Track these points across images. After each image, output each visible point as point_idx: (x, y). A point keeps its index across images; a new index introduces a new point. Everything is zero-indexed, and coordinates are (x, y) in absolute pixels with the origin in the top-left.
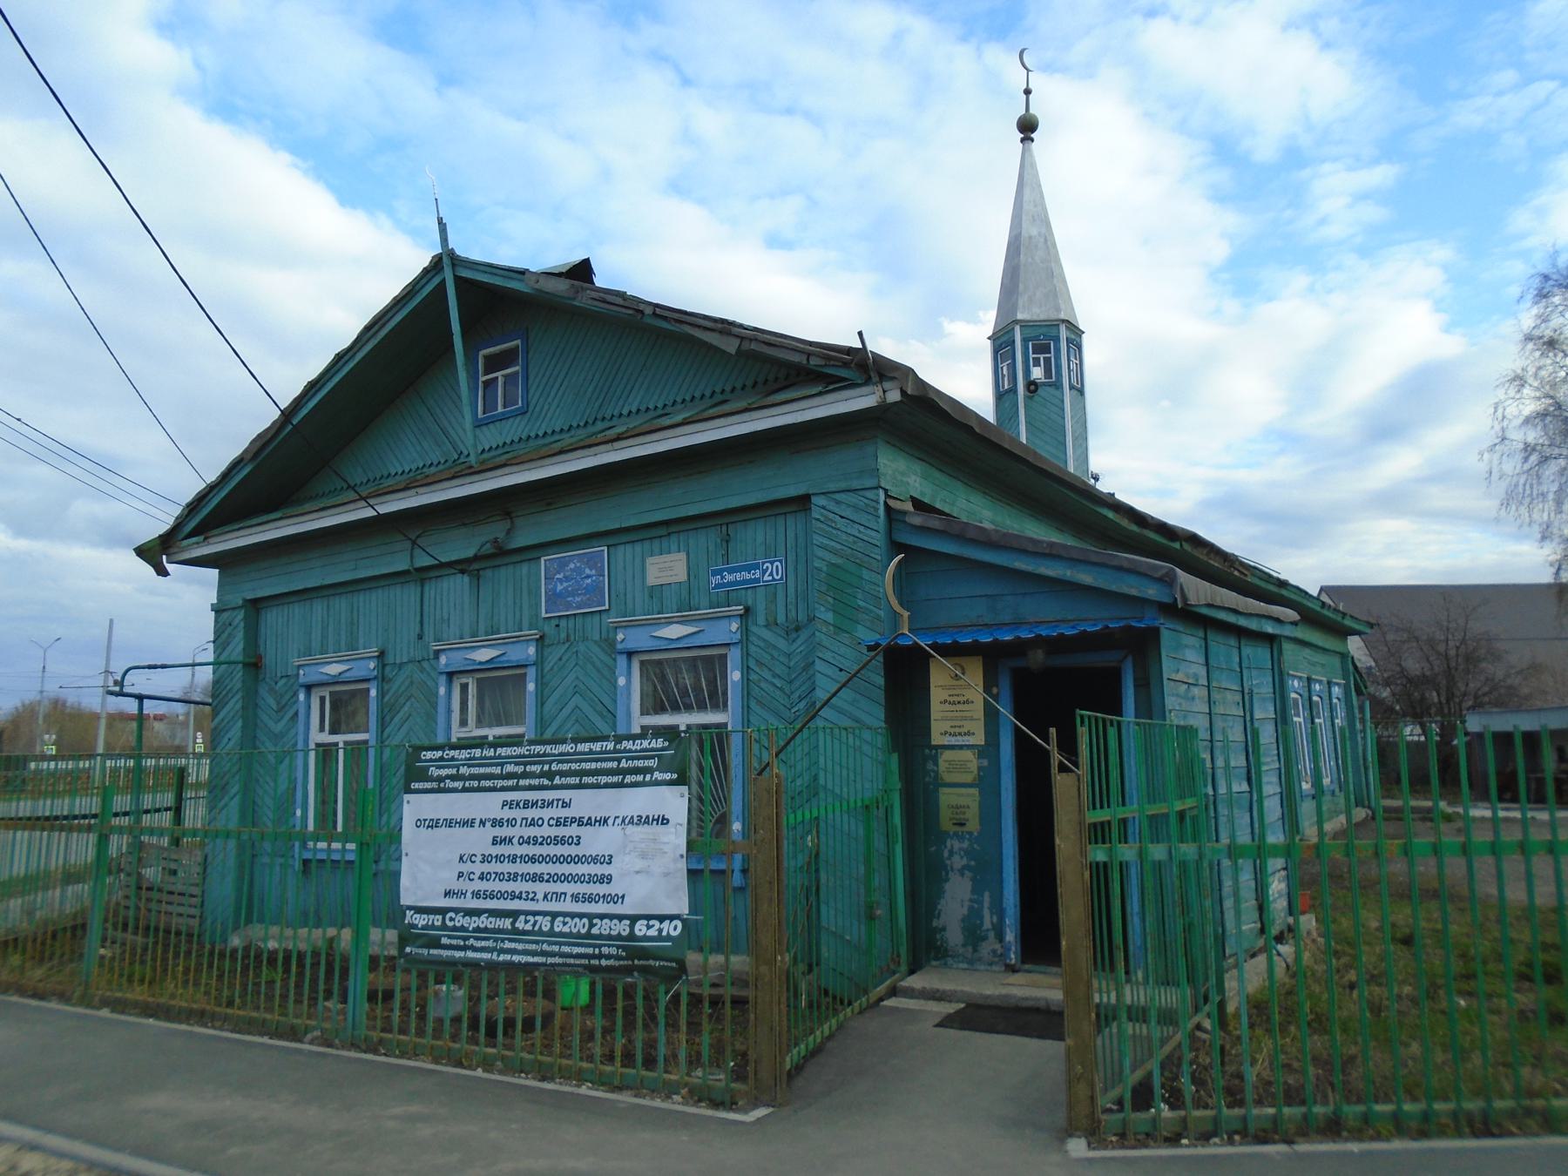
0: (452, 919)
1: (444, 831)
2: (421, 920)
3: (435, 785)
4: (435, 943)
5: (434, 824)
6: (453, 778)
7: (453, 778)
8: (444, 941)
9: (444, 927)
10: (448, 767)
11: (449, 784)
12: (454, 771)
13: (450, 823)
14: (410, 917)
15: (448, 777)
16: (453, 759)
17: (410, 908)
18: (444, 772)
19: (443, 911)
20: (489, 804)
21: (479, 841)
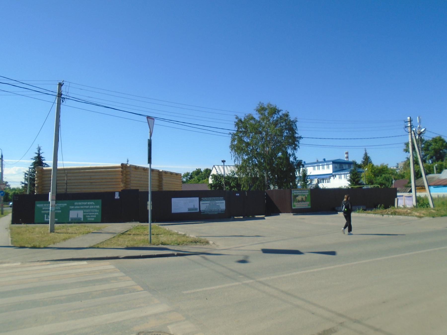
20: (209, 202)
21: (208, 205)
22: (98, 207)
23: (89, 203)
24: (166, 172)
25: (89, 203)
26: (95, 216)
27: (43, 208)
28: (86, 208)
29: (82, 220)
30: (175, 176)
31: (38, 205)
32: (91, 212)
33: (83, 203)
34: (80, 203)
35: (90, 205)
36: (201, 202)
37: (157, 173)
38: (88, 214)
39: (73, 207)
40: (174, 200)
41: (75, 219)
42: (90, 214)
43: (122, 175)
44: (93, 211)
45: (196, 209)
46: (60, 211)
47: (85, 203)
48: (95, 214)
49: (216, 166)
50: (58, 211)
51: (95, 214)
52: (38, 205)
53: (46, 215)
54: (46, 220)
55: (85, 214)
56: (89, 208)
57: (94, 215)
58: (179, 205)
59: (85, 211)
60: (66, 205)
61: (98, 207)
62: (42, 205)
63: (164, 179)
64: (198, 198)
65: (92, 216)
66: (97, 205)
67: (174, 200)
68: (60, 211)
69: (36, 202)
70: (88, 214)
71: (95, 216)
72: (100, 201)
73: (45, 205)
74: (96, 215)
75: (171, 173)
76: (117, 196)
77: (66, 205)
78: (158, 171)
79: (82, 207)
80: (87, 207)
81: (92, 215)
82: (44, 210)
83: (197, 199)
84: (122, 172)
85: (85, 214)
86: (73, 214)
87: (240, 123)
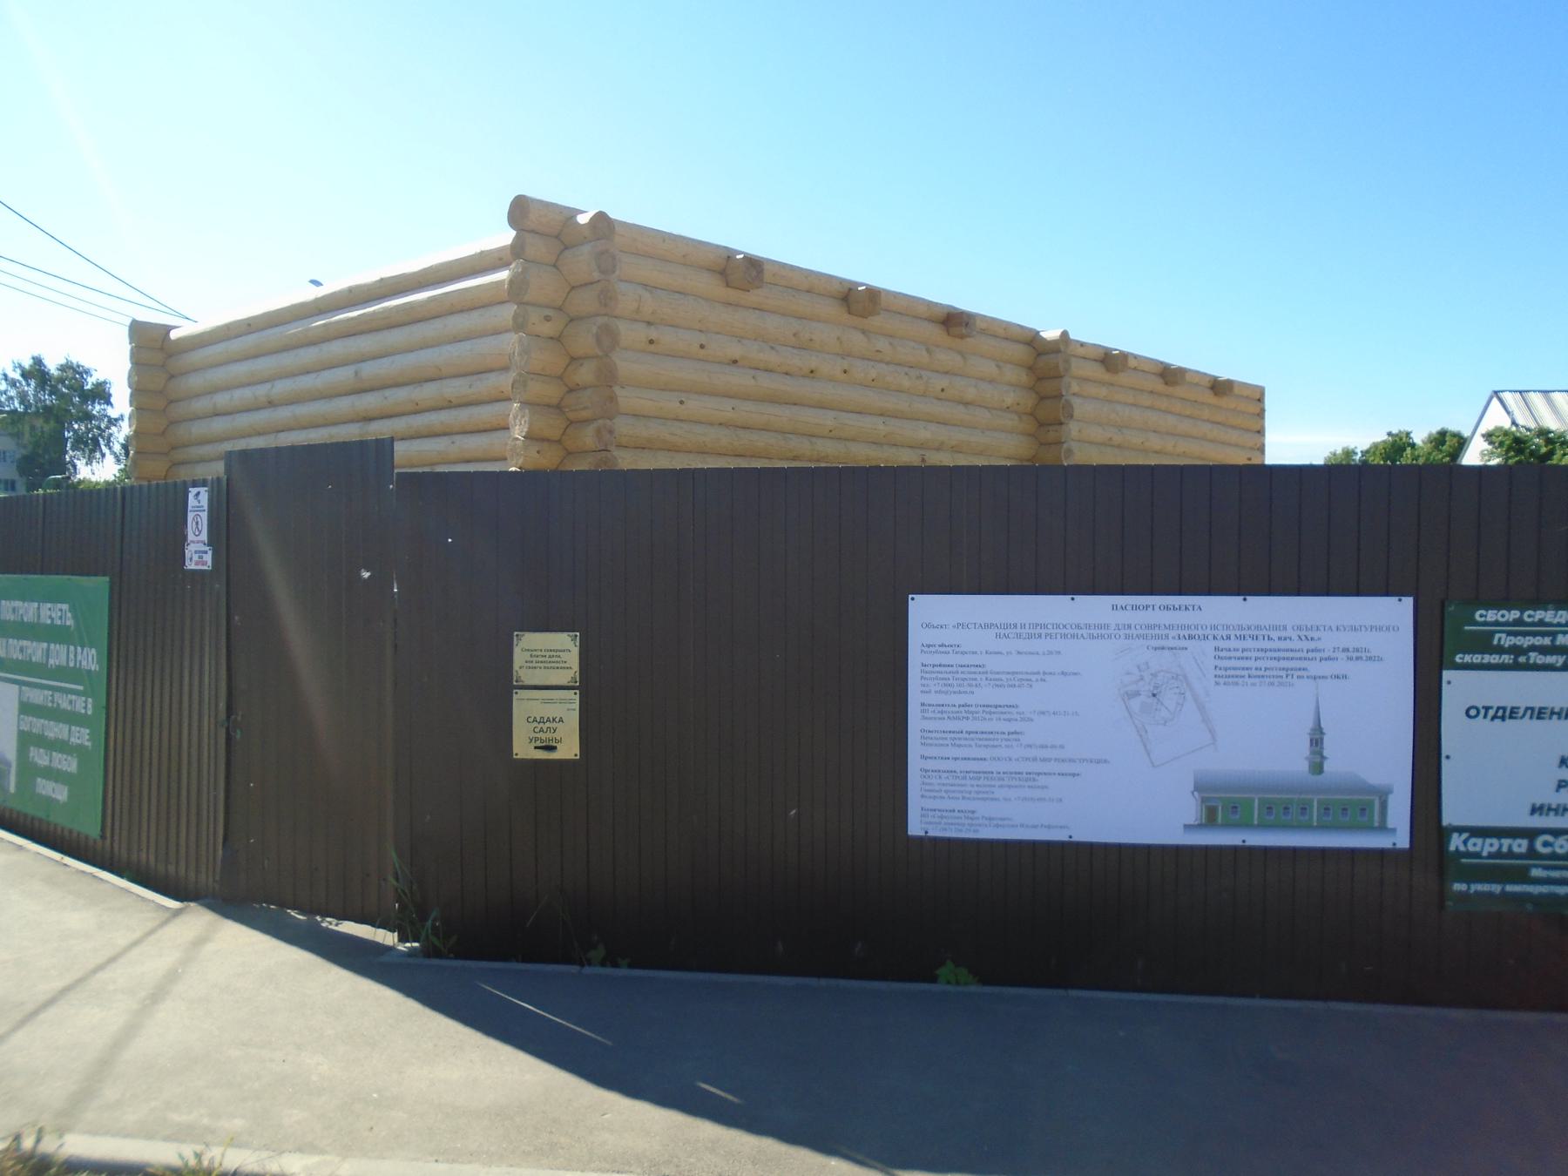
0: (1546, 844)
1: (1527, 725)
2: (1489, 846)
3: (1507, 659)
4: (1522, 876)
5: (1507, 714)
6: (1543, 650)
7: (1543, 650)
8: (1536, 873)
9: (1532, 853)
10: (1534, 634)
11: (1534, 657)
12: (1547, 641)
13: (1540, 714)
14: (1456, 842)
15: (1533, 648)
16: (1541, 623)
17: (1460, 830)
18: (1526, 642)
19: (1531, 834)
24: (1111, 361)
30: (1209, 398)
36: (1459, 688)
37: (1020, 352)
40: (941, 625)
43: (519, 325)
44: (64, 702)
45: (1360, 806)
49: (1507, 397)
58: (1048, 721)
63: (1081, 408)
64: (1397, 612)
67: (941, 625)
75: (1170, 375)
78: (1031, 340)
83: (1392, 617)
84: (516, 288)
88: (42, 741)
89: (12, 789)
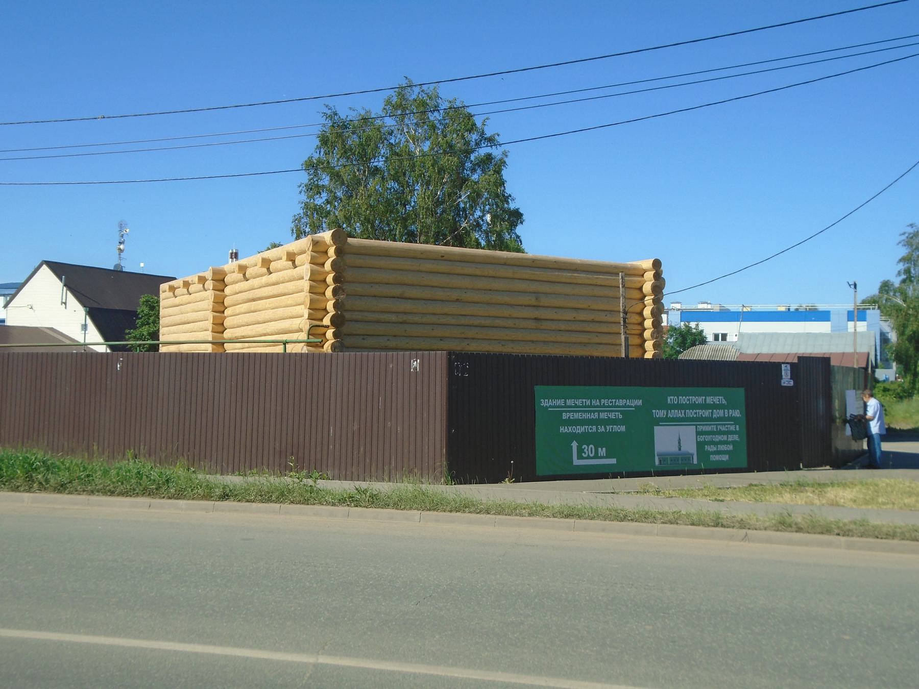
22: (736, 413)
23: (709, 400)
25: (709, 400)
26: (731, 447)
27: (565, 416)
28: (702, 419)
29: (695, 462)
31: (545, 403)
32: (720, 433)
33: (693, 399)
34: (684, 400)
35: (714, 406)
38: (708, 438)
39: (661, 413)
41: (674, 458)
42: (717, 438)
44: (723, 429)
46: (623, 428)
47: (700, 400)
48: (731, 438)
50: (617, 428)
51: (731, 438)
52: (545, 403)
53: (575, 444)
54: (576, 462)
55: (701, 438)
56: (710, 419)
57: (726, 443)
59: (700, 428)
60: (640, 402)
61: (736, 413)
62: (560, 402)
65: (721, 447)
66: (734, 408)
68: (623, 428)
69: (538, 389)
70: (708, 438)
71: (731, 447)
72: (740, 392)
73: (569, 402)
74: (733, 442)
76: (786, 380)
77: (640, 402)
79: (690, 413)
80: (706, 413)
81: (721, 443)
82: (570, 422)
85: (701, 438)
86: (668, 439)
87: (336, 135)
88: (712, 443)
89: (695, 462)
